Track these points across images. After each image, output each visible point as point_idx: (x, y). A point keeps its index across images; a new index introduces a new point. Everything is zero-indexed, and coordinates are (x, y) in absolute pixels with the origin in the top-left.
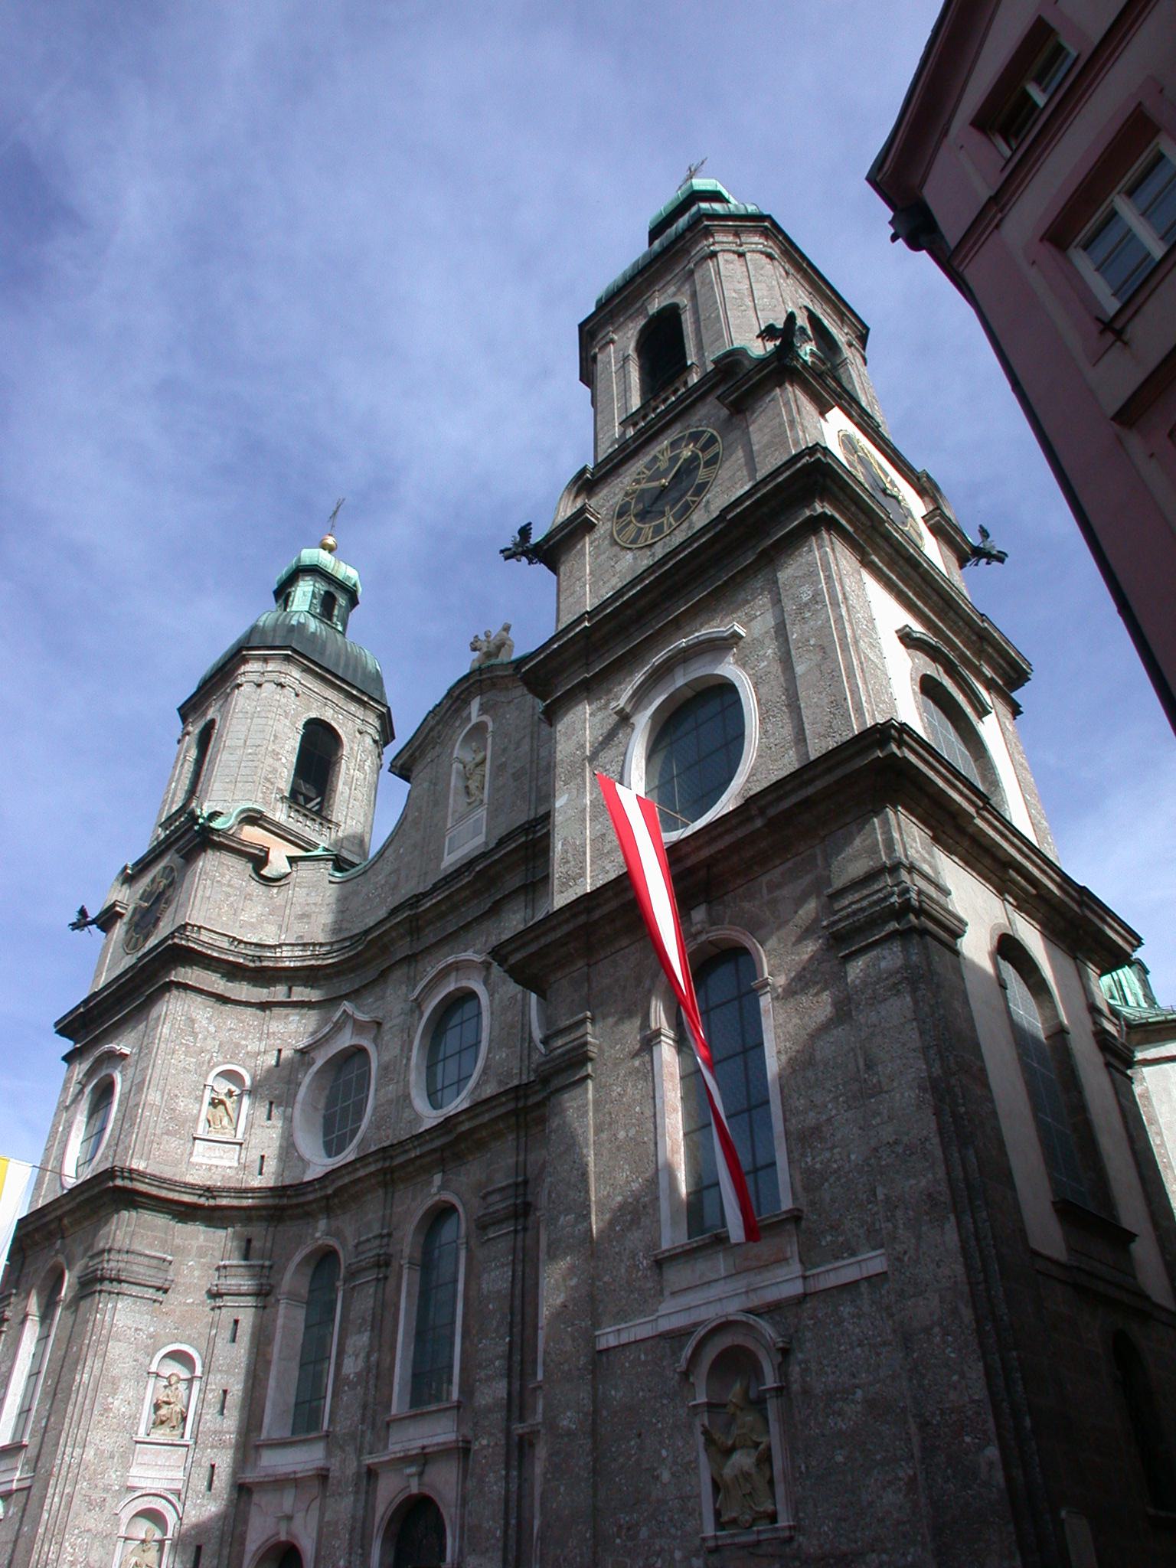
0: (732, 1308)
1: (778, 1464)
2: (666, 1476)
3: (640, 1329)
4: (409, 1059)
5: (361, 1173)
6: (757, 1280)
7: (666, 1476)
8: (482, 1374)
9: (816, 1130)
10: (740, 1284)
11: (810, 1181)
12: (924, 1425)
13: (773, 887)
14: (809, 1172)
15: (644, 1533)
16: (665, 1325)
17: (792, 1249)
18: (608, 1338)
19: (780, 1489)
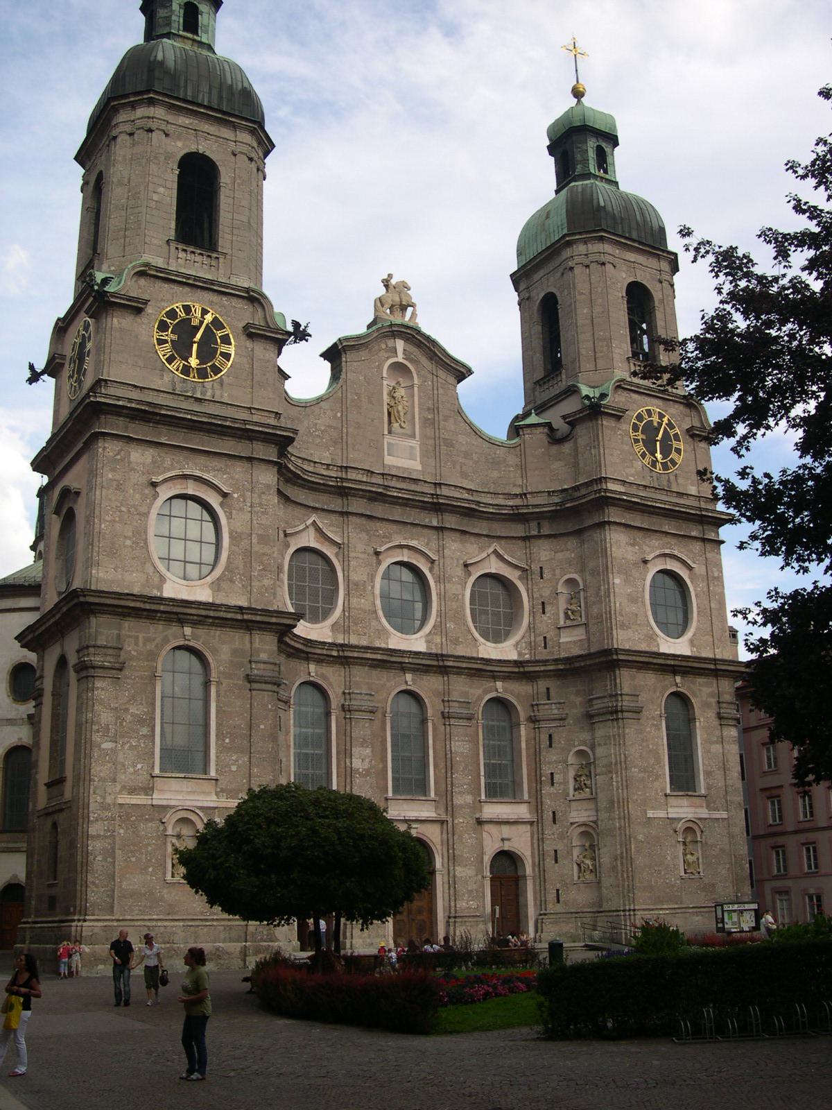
0: (690, 816)
1: (700, 860)
2: (669, 858)
3: (661, 814)
4: (373, 587)
5: (368, 656)
6: (697, 810)
7: (669, 858)
8: (457, 790)
9: (711, 772)
10: (691, 810)
11: (709, 787)
12: (735, 857)
13: (700, 685)
14: (708, 784)
15: (663, 873)
16: (670, 816)
17: (704, 805)
18: (650, 814)
19: (701, 866)
